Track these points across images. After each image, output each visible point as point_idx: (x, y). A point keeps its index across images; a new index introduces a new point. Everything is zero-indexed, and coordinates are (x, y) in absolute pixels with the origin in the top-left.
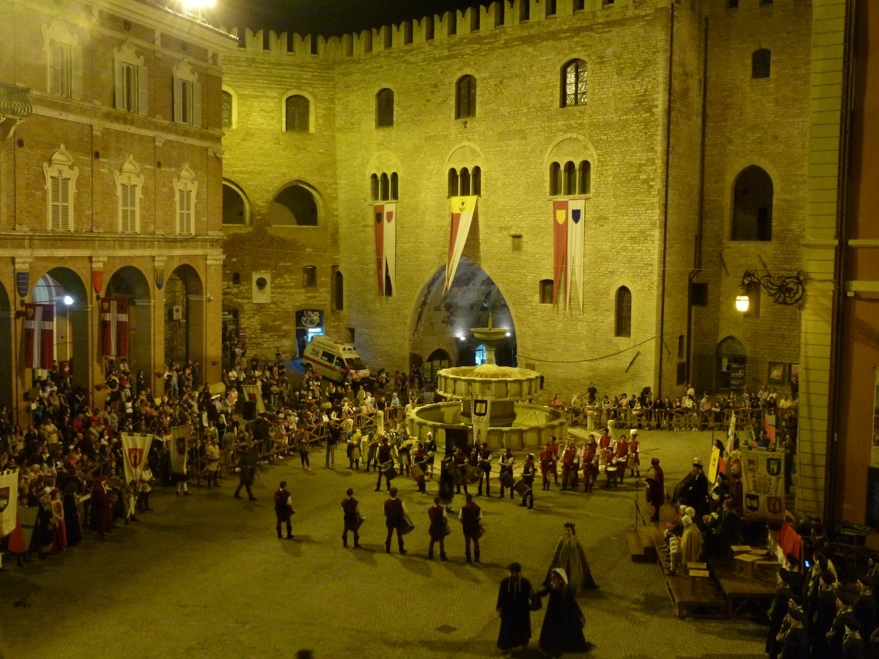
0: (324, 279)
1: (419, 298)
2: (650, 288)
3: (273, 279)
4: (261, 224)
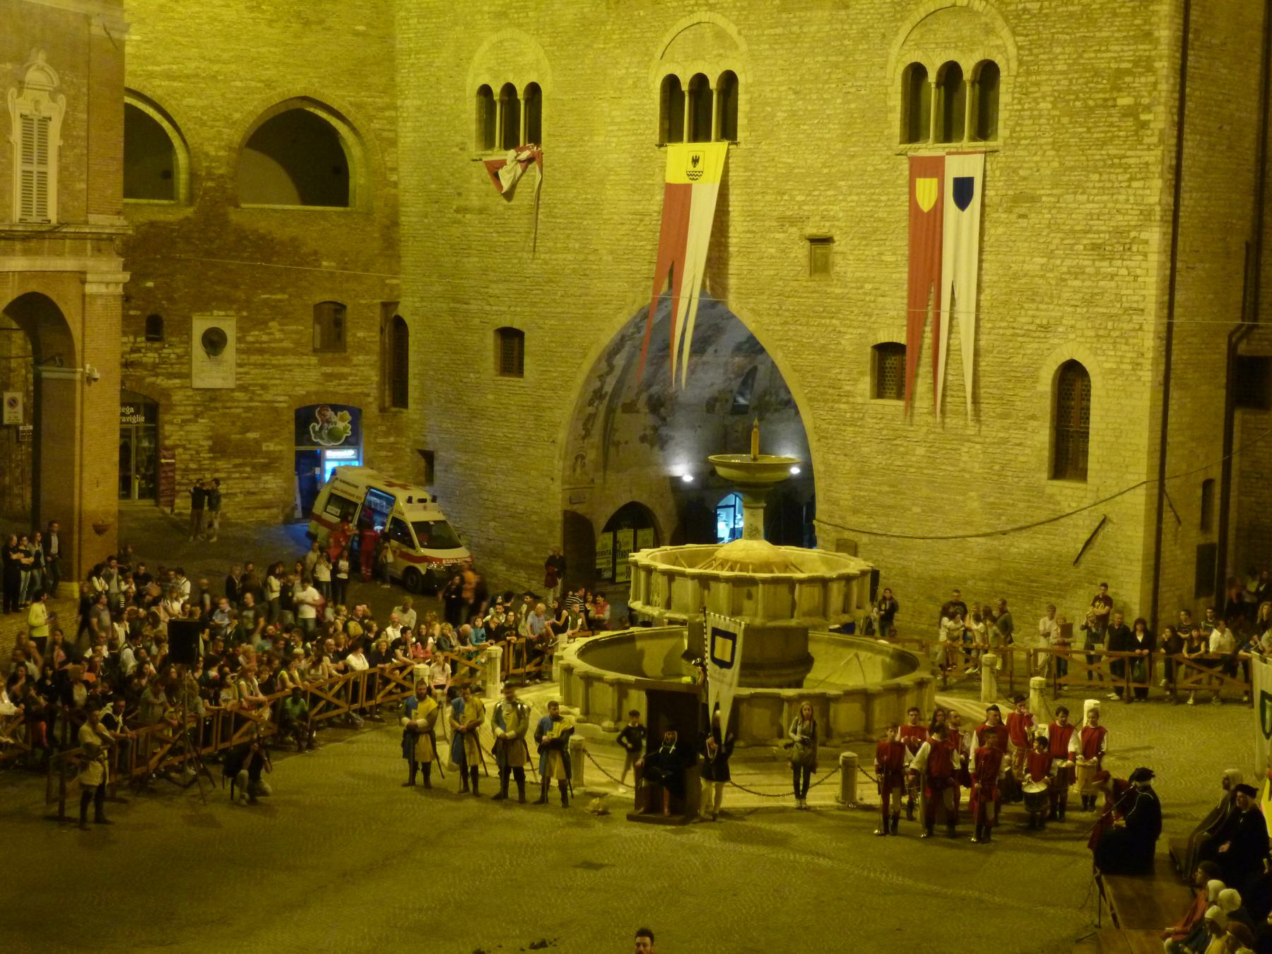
0: (365, 334)
1: (588, 381)
2: (1136, 365)
3: (242, 330)
4: (215, 204)
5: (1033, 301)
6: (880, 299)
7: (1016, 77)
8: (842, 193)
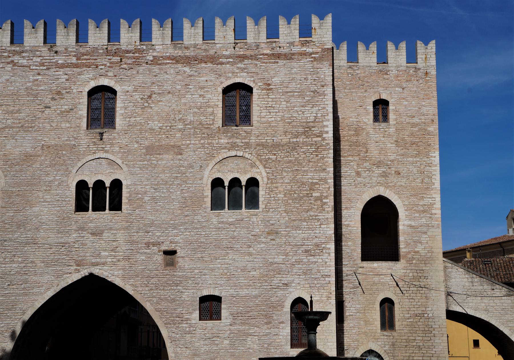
2: (329, 298)
5: (279, 274)
6: (204, 276)
7: (267, 184)
8: (181, 232)
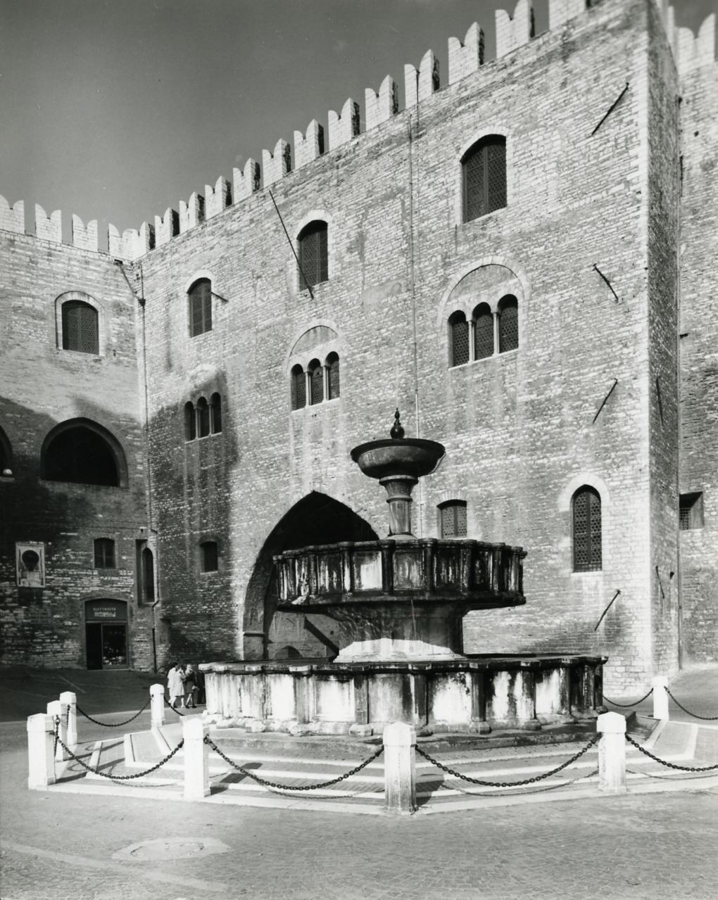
3: (49, 552)
